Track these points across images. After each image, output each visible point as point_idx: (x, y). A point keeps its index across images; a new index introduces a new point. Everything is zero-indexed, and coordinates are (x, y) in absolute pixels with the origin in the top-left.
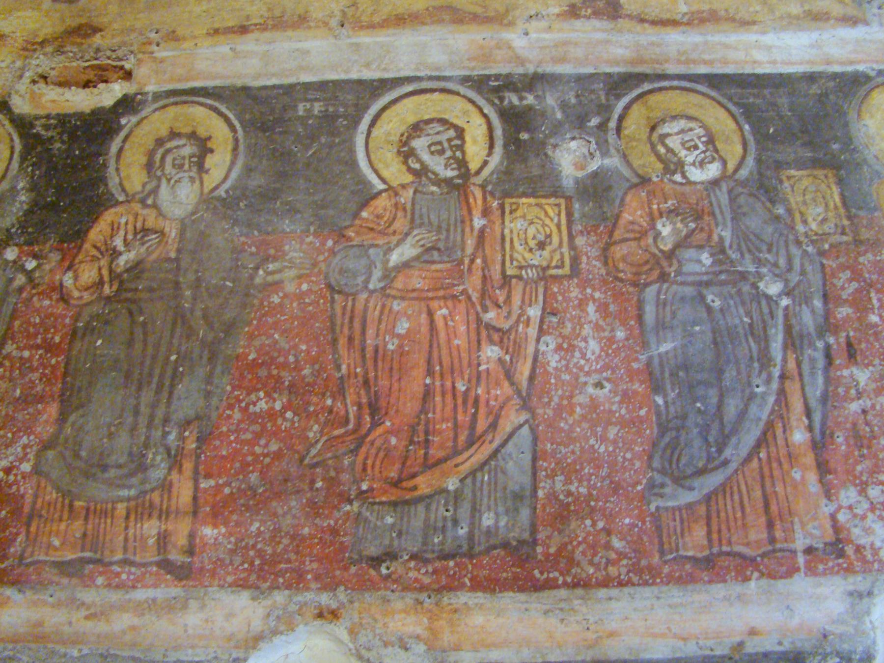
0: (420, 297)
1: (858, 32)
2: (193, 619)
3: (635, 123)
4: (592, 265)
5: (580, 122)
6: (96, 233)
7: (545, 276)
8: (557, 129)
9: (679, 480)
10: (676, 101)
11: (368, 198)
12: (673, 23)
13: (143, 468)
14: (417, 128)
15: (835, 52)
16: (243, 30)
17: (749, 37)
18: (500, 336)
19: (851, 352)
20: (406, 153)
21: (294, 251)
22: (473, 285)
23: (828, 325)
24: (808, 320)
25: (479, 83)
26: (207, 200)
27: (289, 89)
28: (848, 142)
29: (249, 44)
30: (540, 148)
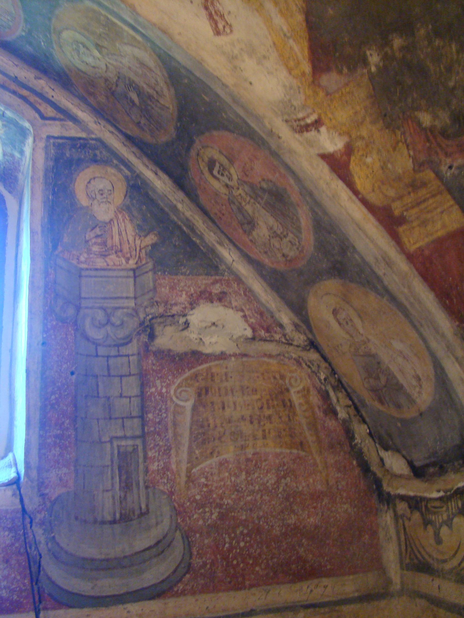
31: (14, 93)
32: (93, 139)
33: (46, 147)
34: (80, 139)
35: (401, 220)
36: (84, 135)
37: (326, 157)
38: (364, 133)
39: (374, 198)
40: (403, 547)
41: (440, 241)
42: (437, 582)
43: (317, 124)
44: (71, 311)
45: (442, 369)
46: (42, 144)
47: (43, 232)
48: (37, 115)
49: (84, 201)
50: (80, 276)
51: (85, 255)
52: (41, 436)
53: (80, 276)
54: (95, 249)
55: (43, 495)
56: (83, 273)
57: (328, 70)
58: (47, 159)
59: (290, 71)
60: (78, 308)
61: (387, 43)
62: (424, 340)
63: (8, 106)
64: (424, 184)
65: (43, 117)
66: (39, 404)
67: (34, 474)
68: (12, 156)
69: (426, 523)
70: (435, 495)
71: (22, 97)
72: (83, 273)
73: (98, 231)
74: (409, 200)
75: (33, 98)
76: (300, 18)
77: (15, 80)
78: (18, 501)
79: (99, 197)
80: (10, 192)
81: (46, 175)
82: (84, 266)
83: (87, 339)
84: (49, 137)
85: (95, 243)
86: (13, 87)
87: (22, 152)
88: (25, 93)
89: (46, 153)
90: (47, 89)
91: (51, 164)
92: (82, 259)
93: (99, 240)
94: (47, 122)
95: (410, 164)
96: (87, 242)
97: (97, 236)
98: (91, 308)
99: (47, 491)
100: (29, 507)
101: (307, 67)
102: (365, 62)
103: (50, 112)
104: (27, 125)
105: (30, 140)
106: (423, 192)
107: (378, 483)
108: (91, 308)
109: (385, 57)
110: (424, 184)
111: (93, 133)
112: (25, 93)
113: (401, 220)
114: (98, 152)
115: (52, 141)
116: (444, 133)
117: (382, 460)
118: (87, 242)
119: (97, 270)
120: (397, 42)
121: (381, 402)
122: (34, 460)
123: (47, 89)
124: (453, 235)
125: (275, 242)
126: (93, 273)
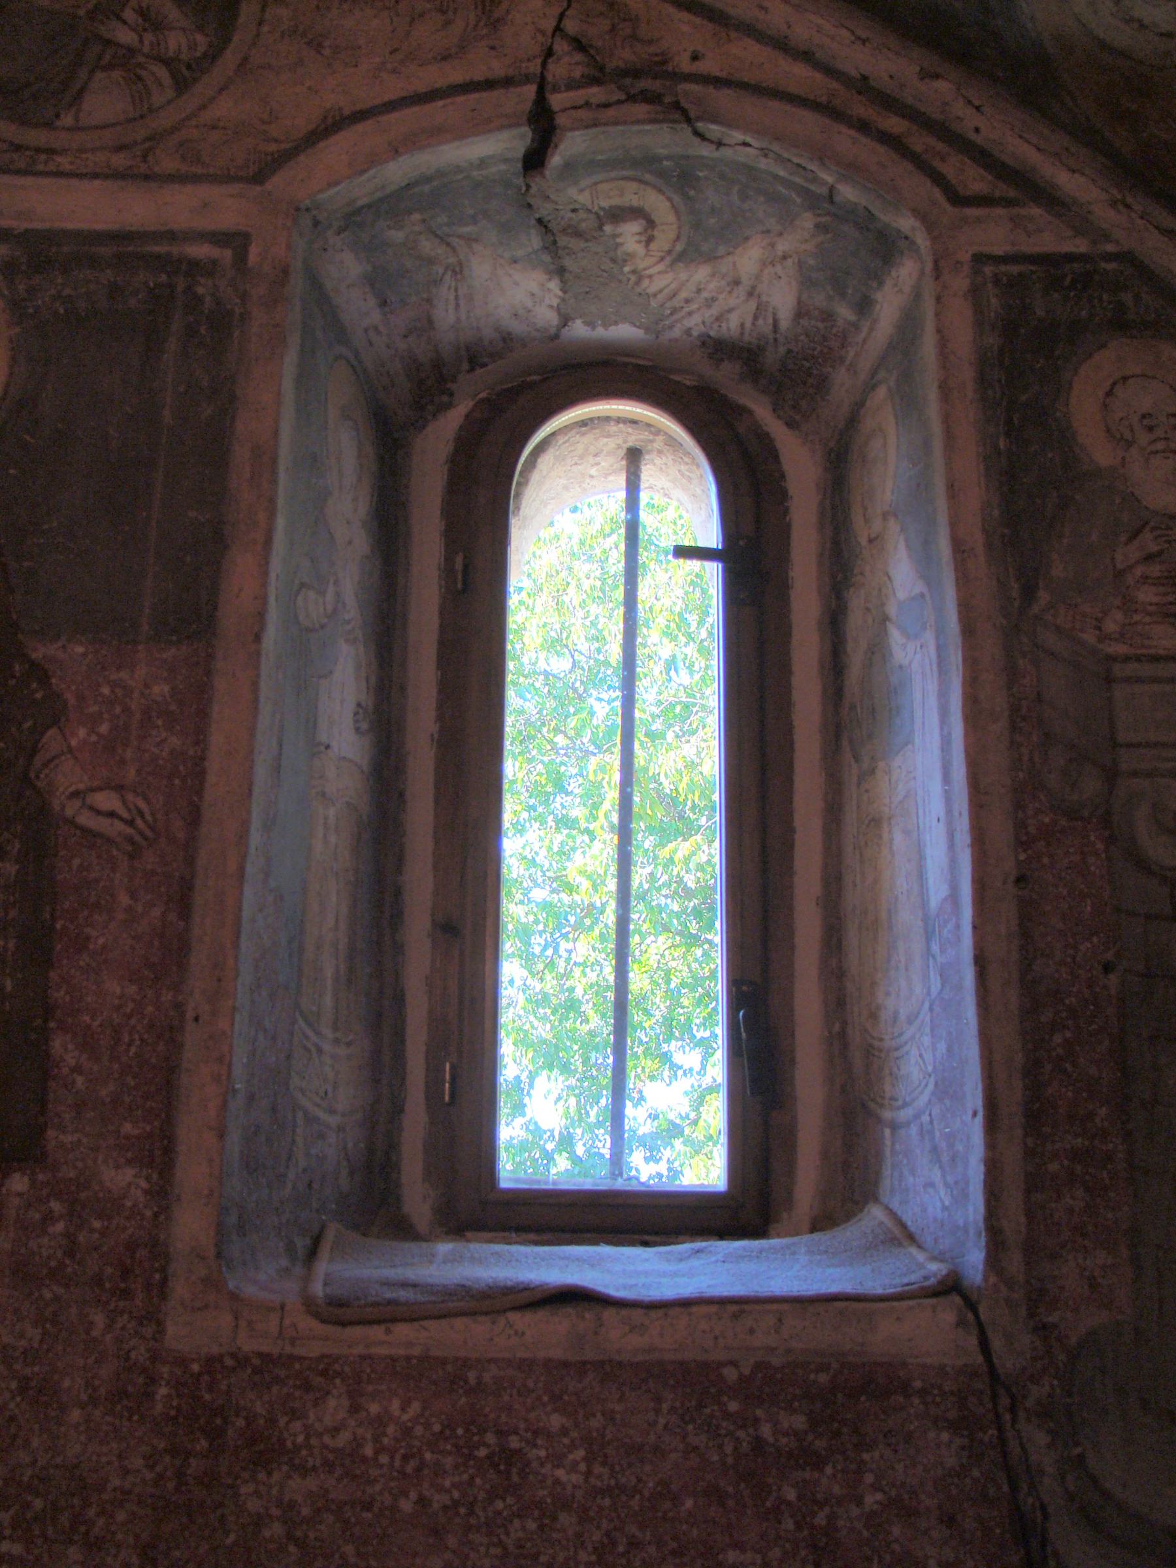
31: (863, 127)
32: (1109, 257)
33: (975, 292)
34: (1070, 258)
36: (1080, 246)
44: (1091, 785)
46: (960, 283)
47: (989, 546)
48: (937, 194)
49: (1102, 454)
50: (1109, 680)
51: (1119, 616)
52: (1029, 1153)
53: (1109, 680)
54: (1147, 595)
55: (1042, 1329)
56: (1118, 670)
58: (979, 324)
60: (1111, 775)
63: (851, 169)
65: (957, 199)
66: (1019, 1058)
67: (1015, 1262)
68: (828, 316)
71: (887, 139)
72: (1118, 670)
73: (1149, 541)
75: (920, 142)
77: (862, 85)
78: (973, 1341)
79: (1143, 438)
80: (791, 424)
81: (982, 380)
82: (1120, 649)
83: (1142, 865)
84: (980, 259)
85: (1145, 578)
86: (860, 108)
87: (864, 306)
88: (894, 124)
89: (978, 310)
90: (959, 109)
91: (993, 341)
92: (1111, 627)
93: (1155, 570)
94: (972, 212)
96: (1119, 574)
97: (1149, 558)
98: (1150, 774)
99: (1053, 1318)
100: (1007, 1363)
103: (975, 180)
104: (906, 223)
105: (906, 272)
108: (1150, 774)
111: (1107, 237)
112: (894, 124)
114: (1127, 298)
115: (988, 270)
118: (1119, 574)
119: (1155, 659)
122: (1014, 1223)
123: (959, 109)
126: (1147, 670)
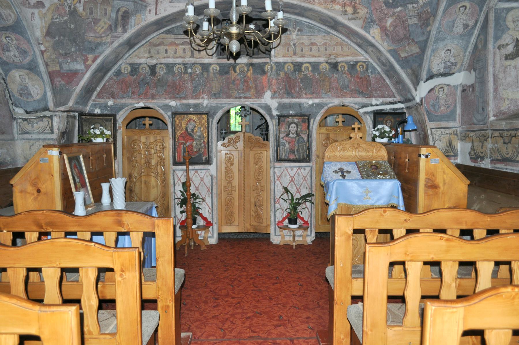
0: (179, 81)
1: (212, 59)
2: (166, 101)
3: (194, 68)
4: (190, 79)
5: (190, 68)
6: (156, 75)
7: (187, 80)
8: (188, 68)
9: (194, 93)
10: (197, 66)
11: (175, 74)
12: (198, 58)
13: (162, 92)
14: (178, 68)
15: (210, 61)
16: (165, 58)
17: (204, 60)
18: (184, 84)
19: (206, 86)
20: (178, 70)
21: (170, 78)
22: (182, 80)
23: (205, 84)
24: (203, 83)
25: (183, 64)
26: (164, 73)
27: (169, 64)
28: (209, 69)
29: (165, 59)
30: (187, 70)
35: (49, 65)
37: (41, 51)
38: (49, 49)
39: (46, 60)
40: (19, 130)
41: (54, 71)
42: (31, 135)
43: (42, 44)
45: (46, 93)
57: (48, 36)
59: (41, 33)
61: (60, 37)
62: (45, 87)
64: (55, 61)
69: (29, 124)
70: (33, 117)
74: (52, 63)
76: (48, 25)
95: (55, 57)
101: (44, 34)
102: (55, 38)
106: (54, 62)
107: (12, 115)
109: (59, 39)
110: (55, 61)
113: (49, 65)
116: (62, 55)
117: (14, 110)
120: (62, 38)
121: (21, 96)
124: (56, 71)
125: (13, 58)
